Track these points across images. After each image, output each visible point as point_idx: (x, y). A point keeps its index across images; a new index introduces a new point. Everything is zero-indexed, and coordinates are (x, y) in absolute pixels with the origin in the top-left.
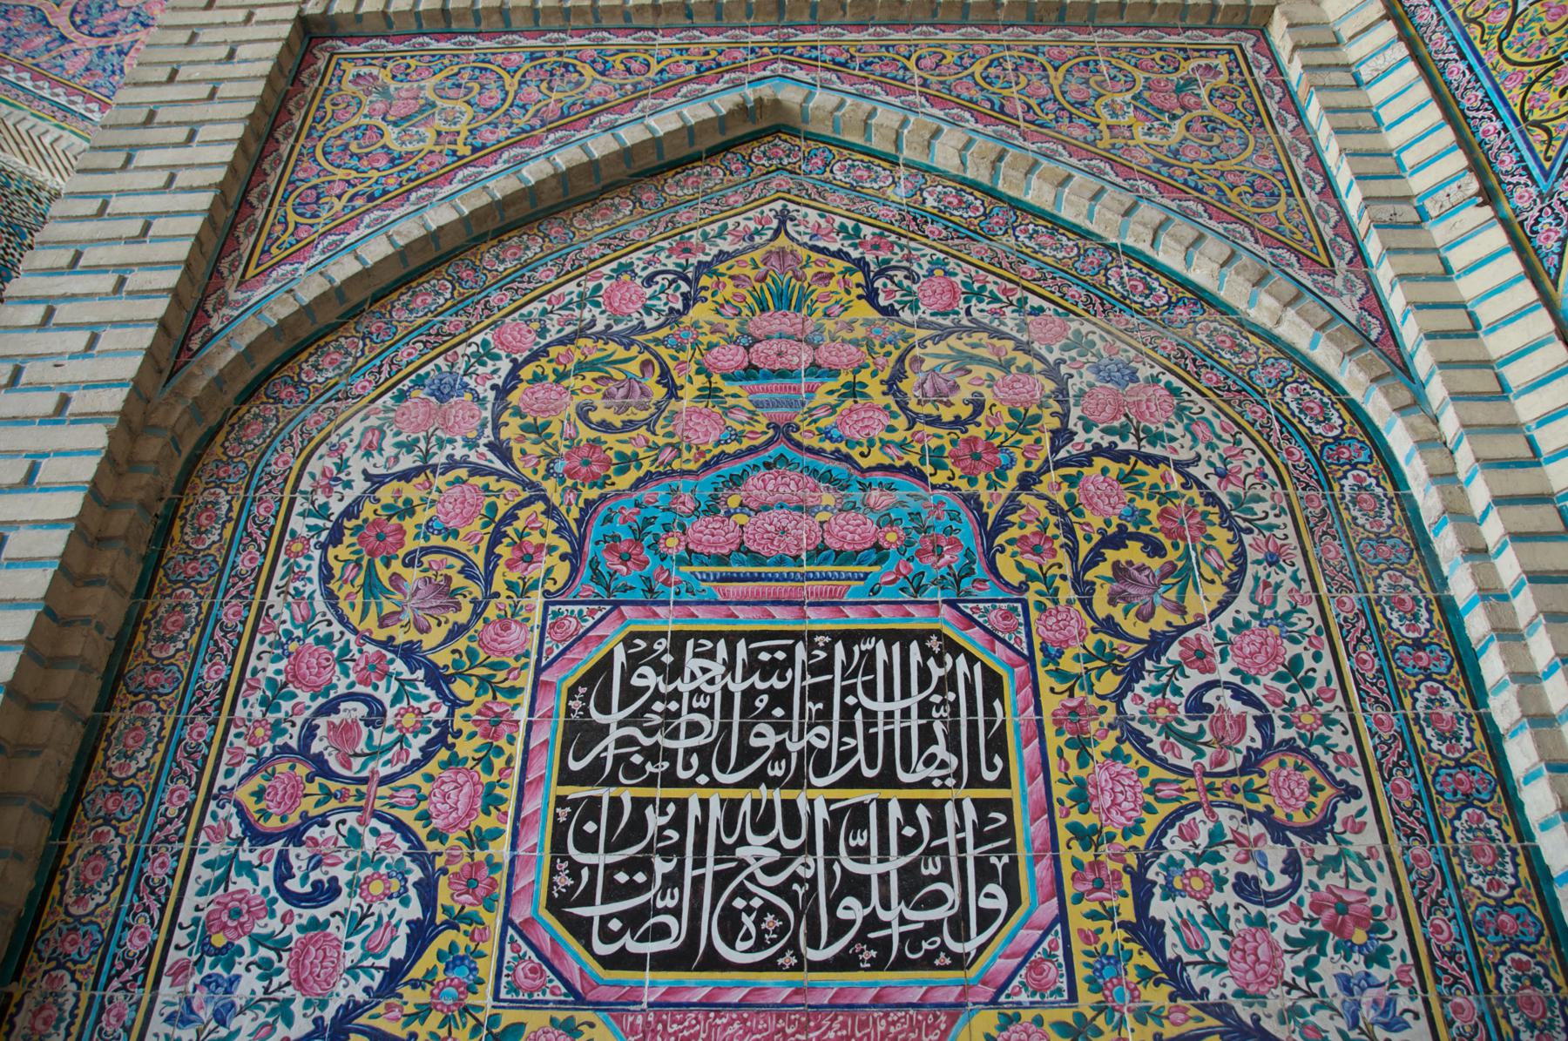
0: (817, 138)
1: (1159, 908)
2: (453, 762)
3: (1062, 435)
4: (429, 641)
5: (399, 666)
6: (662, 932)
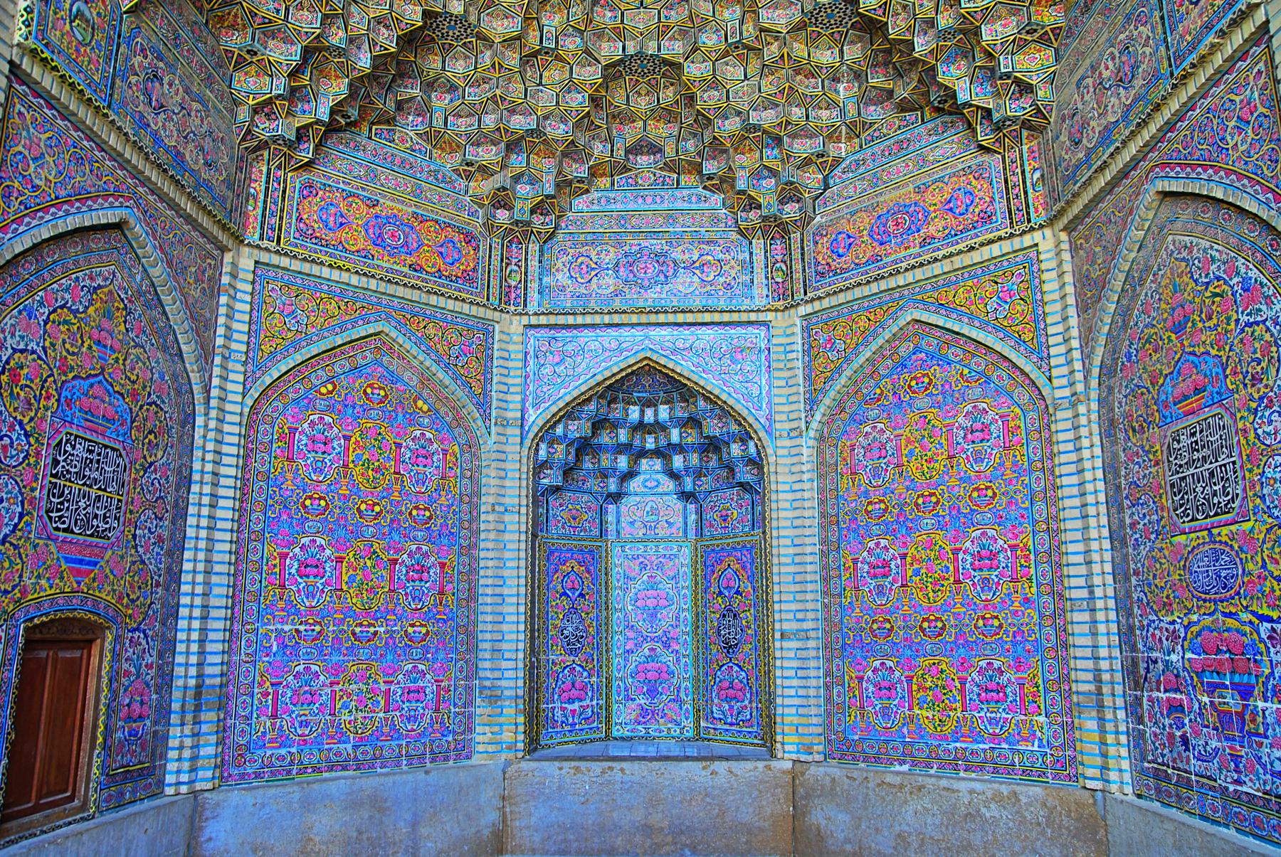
0: (125, 236)
1: (138, 532)
2: (29, 464)
3: (149, 394)
4: (26, 420)
5: (17, 427)
6: (64, 523)
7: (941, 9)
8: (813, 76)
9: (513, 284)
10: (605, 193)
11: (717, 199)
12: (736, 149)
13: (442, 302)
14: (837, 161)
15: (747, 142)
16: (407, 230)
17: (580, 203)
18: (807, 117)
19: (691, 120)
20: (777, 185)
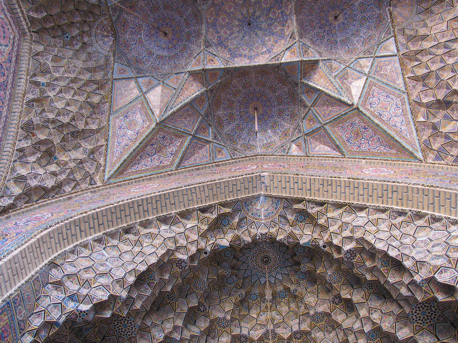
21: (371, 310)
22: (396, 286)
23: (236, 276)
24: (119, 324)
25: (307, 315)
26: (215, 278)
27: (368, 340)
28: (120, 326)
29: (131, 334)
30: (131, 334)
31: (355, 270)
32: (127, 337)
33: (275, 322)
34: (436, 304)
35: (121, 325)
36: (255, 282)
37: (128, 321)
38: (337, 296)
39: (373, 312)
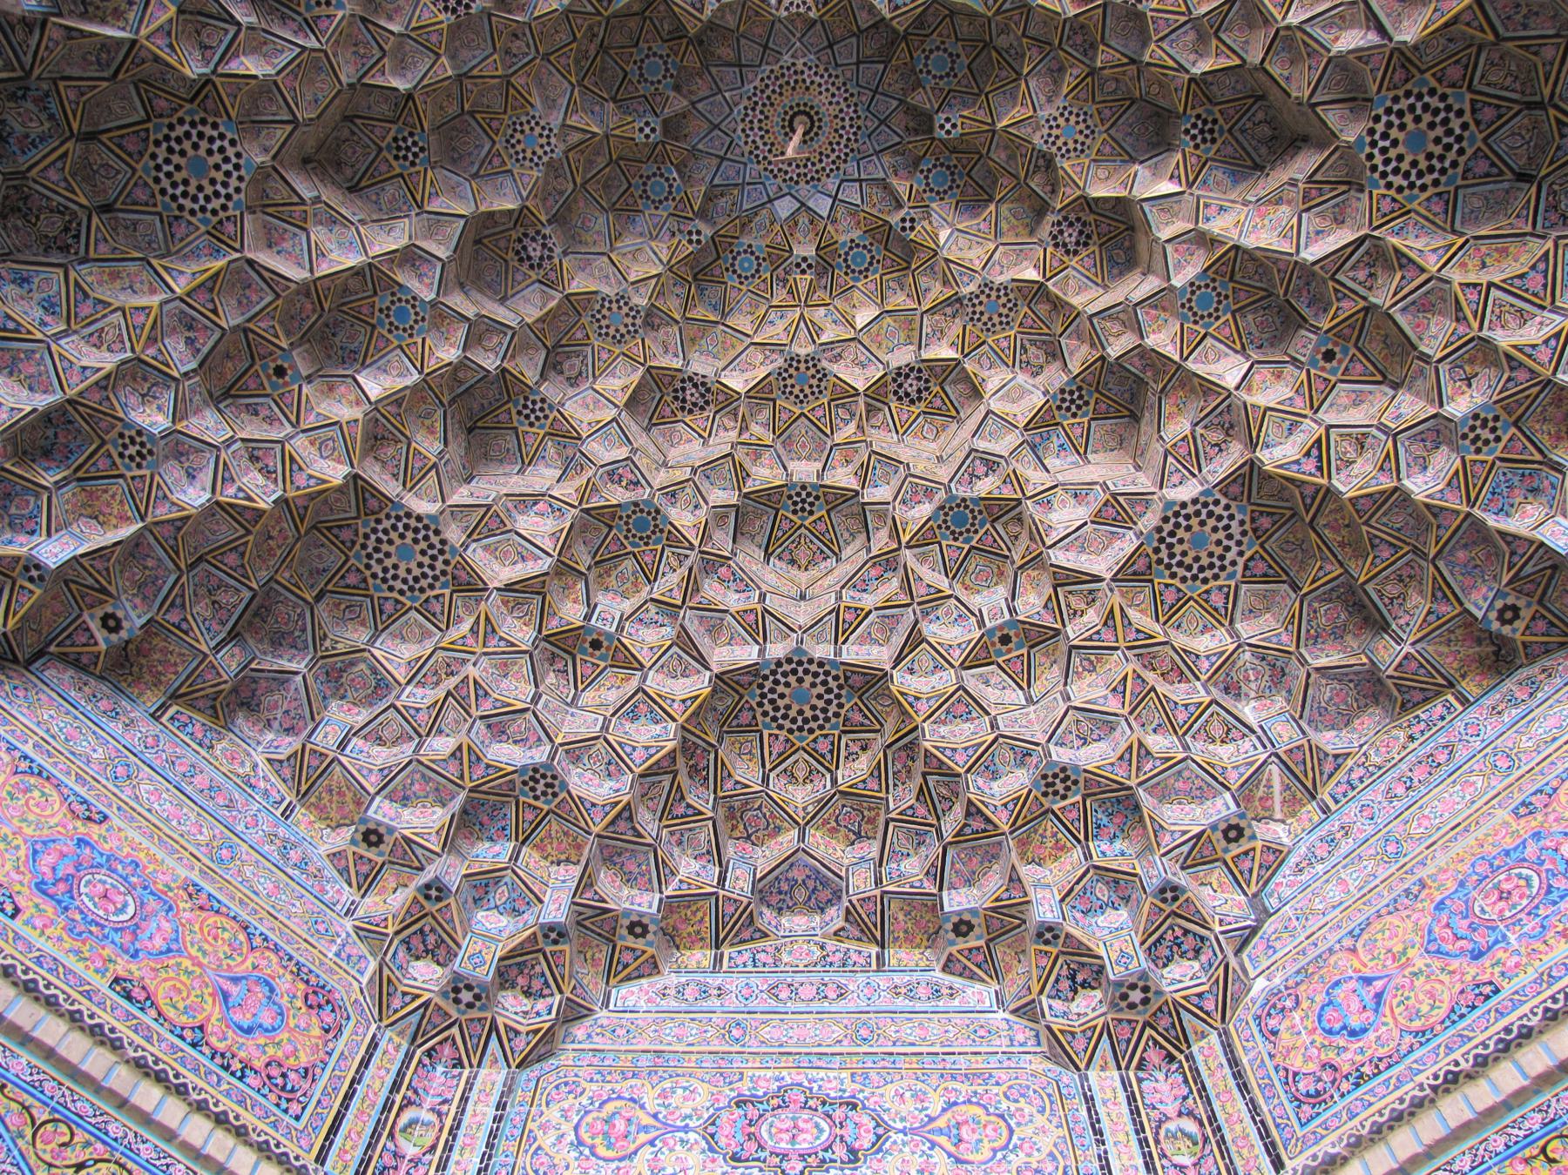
7: (1448, 389)
8: (1182, 677)
9: (410, 1151)
10: (699, 977)
11: (978, 994)
12: (1023, 844)
13: (172, 1112)
14: (1277, 855)
15: (1049, 825)
16: (152, 903)
17: (632, 994)
18: (1186, 748)
19: (910, 800)
20: (1134, 918)
21: (1206, 206)
22: (1317, 32)
23: (679, 172)
24: (176, 159)
25: (949, 310)
26: (596, 130)
27: (1184, 318)
28: (178, 168)
29: (224, 208)
30: (224, 208)
31: (1151, 53)
32: (205, 222)
33: (824, 339)
34: (1468, 96)
35: (182, 162)
36: (755, 211)
37: (211, 140)
38: (1072, 217)
39: (1212, 211)
